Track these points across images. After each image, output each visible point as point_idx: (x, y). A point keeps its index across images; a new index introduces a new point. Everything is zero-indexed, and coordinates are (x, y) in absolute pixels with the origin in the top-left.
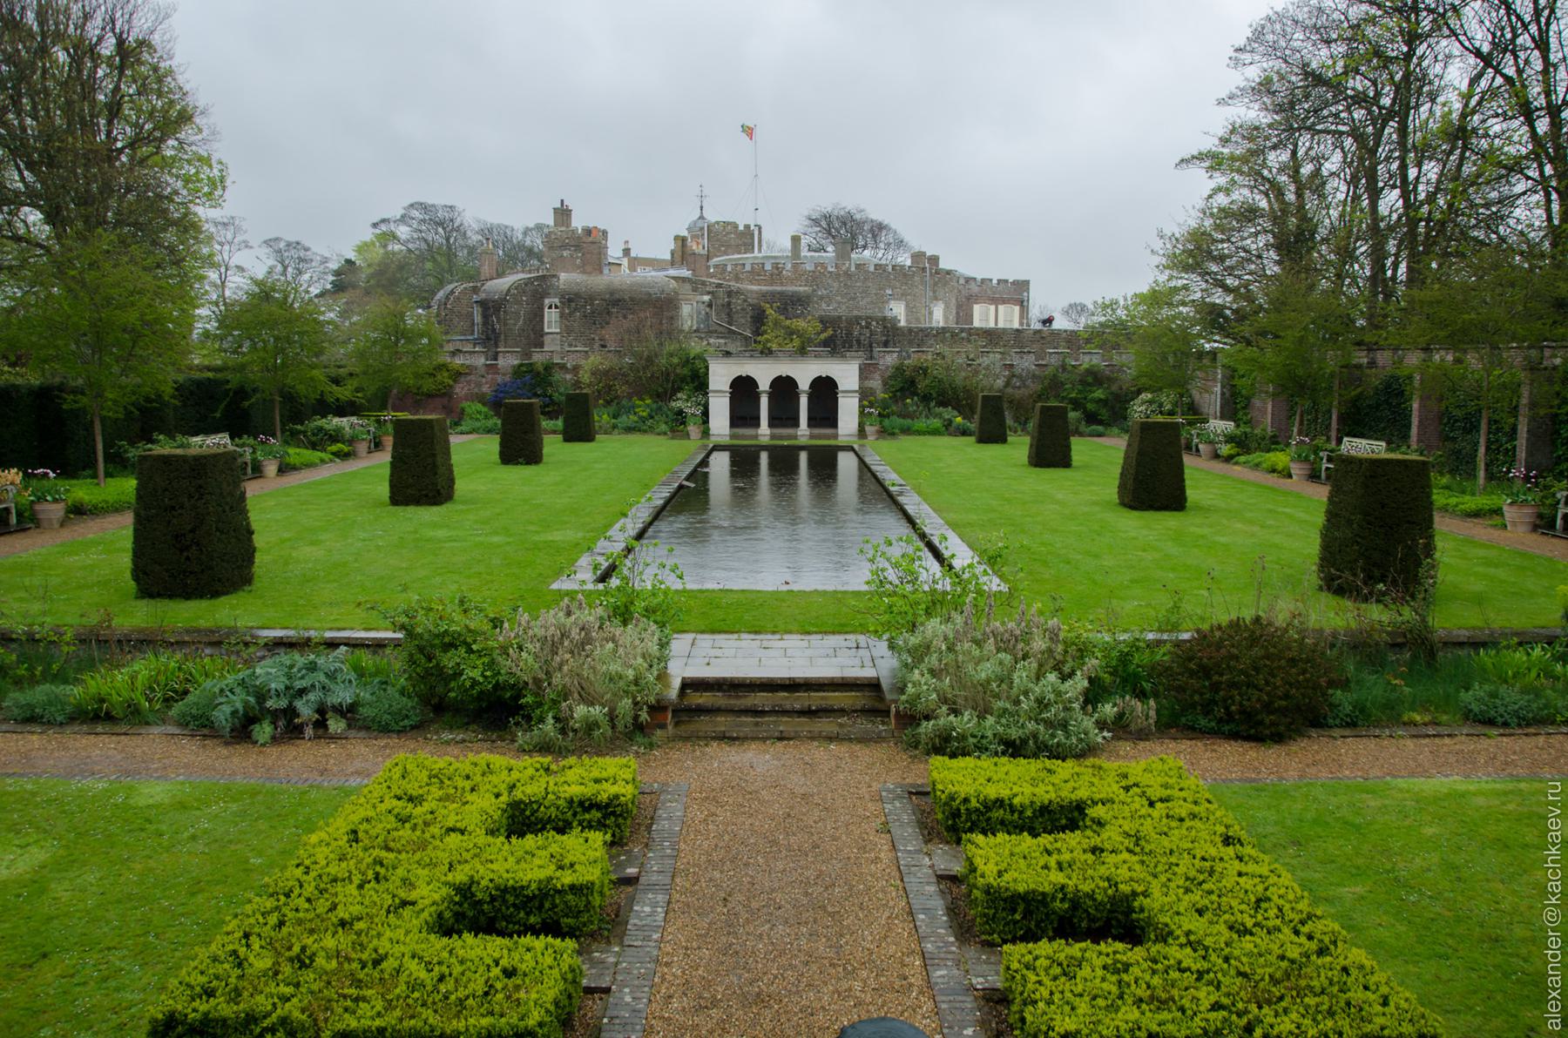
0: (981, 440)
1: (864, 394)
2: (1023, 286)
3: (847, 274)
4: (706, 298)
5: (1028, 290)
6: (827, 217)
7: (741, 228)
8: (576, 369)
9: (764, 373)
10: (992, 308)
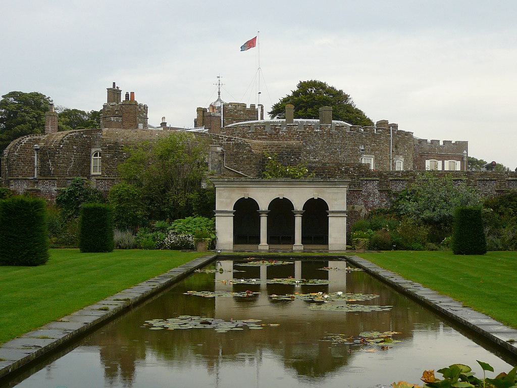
1: (351, 215)
2: (463, 145)
3: (330, 135)
4: (219, 149)
5: (466, 149)
7: (248, 107)
9: (263, 197)
10: (440, 163)
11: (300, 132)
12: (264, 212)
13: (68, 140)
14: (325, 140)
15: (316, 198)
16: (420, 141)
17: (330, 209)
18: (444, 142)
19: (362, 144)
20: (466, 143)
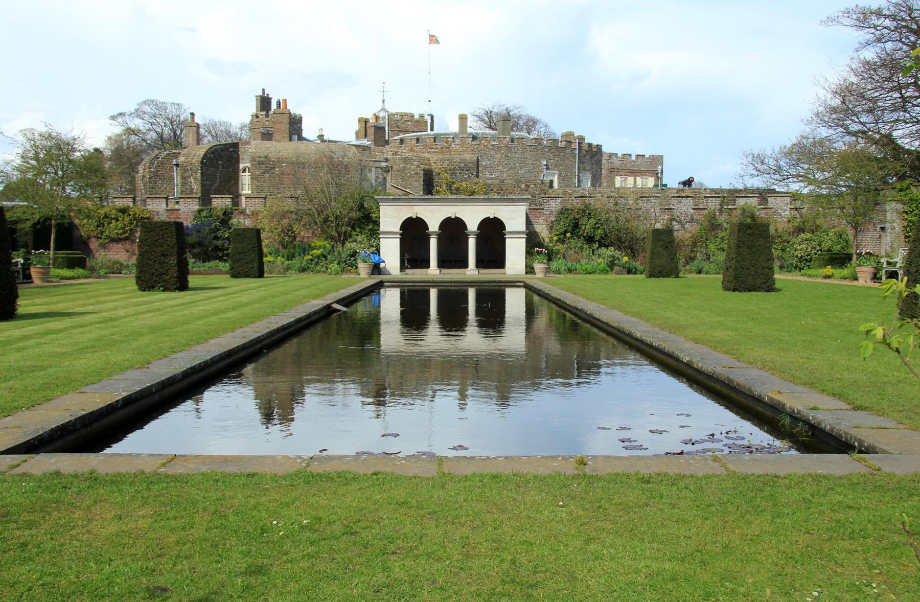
0: (651, 275)
2: (657, 160)
6: (489, 114)
7: (417, 117)
8: (255, 214)
9: (434, 216)
16: (611, 155)
17: (508, 229)
18: (638, 156)
19: (544, 158)
20: (661, 157)
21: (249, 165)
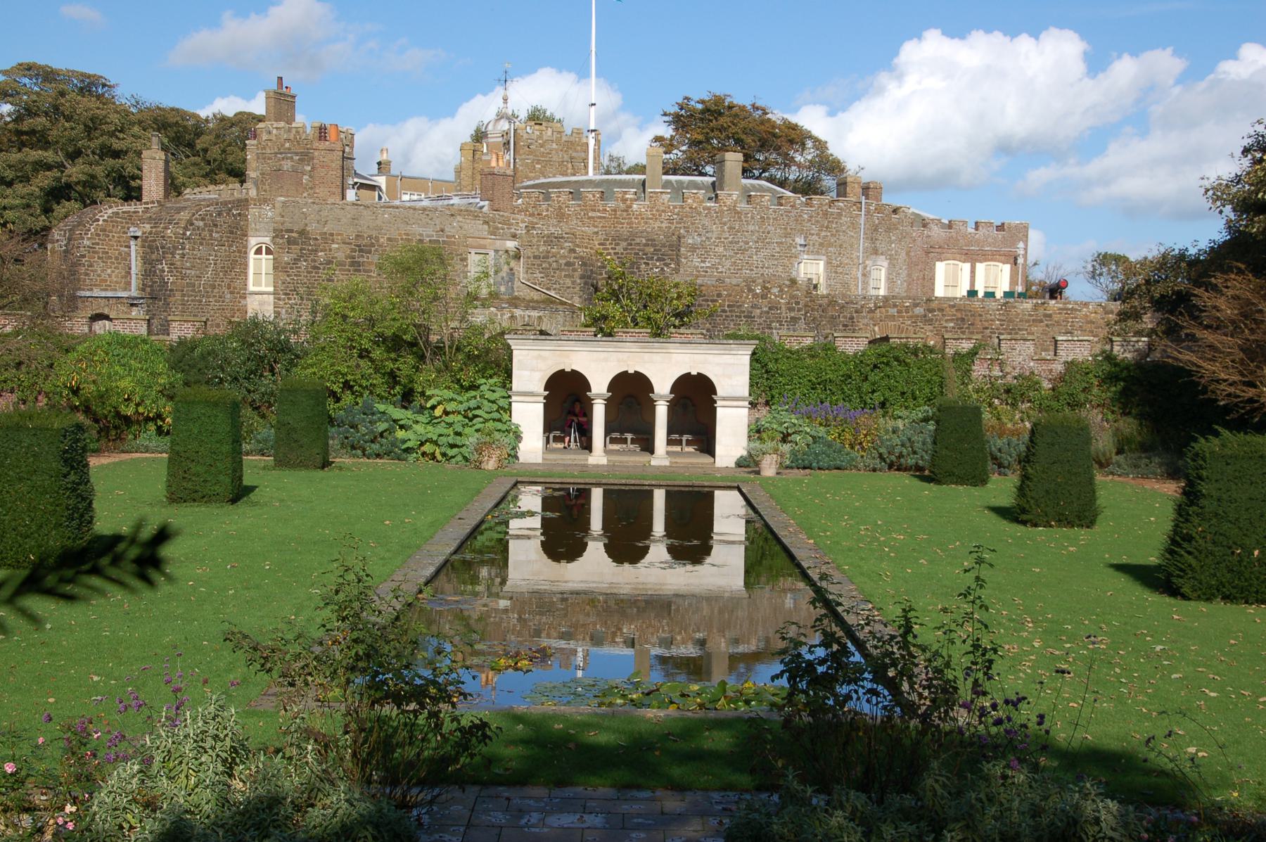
4: (511, 245)
9: (599, 366)
10: (967, 266)
11: (675, 207)
12: (599, 396)
13: (203, 219)
14: (725, 224)
15: (694, 373)
17: (720, 392)
21: (267, 240)
